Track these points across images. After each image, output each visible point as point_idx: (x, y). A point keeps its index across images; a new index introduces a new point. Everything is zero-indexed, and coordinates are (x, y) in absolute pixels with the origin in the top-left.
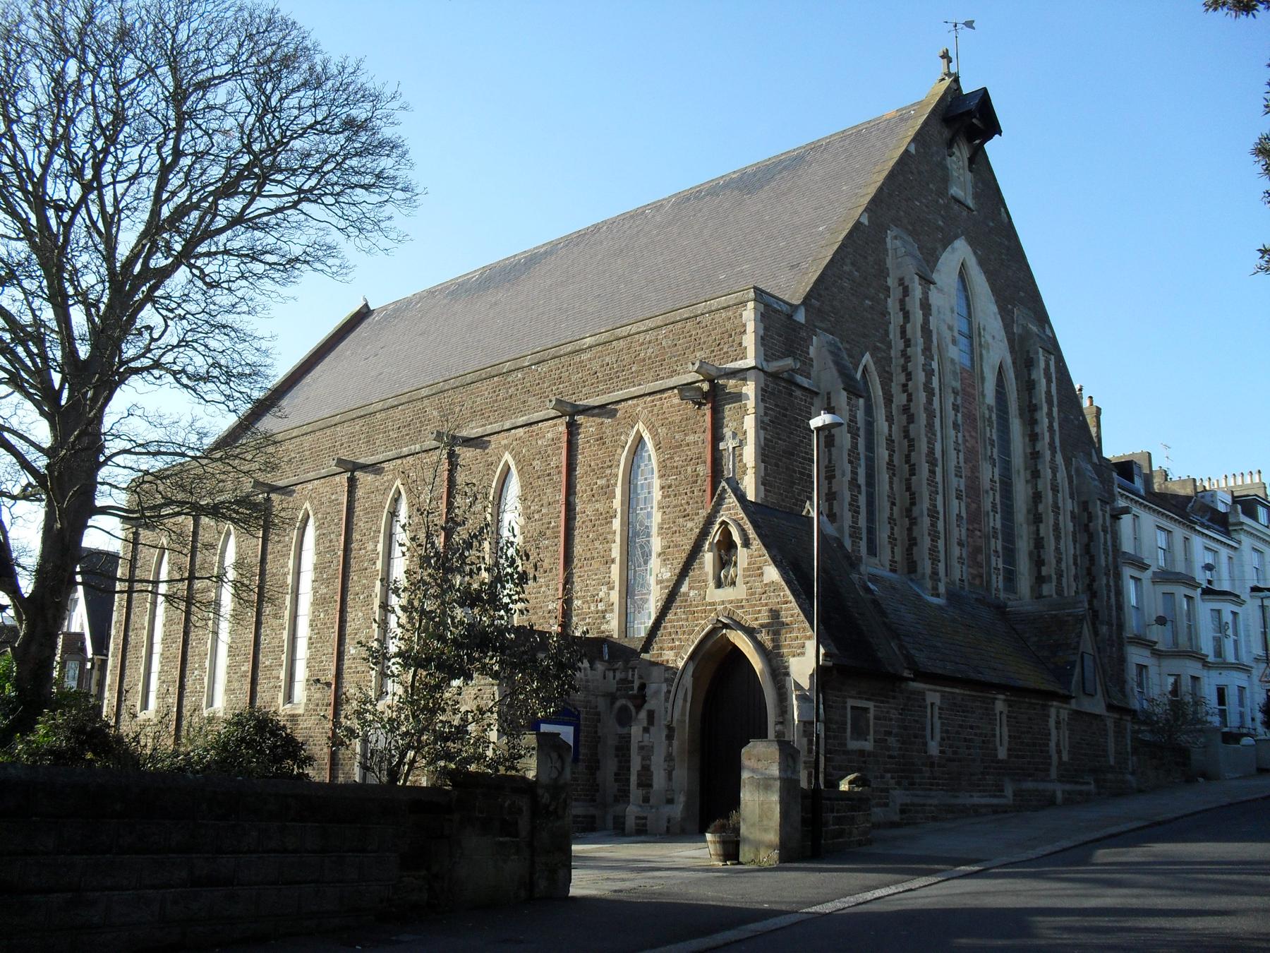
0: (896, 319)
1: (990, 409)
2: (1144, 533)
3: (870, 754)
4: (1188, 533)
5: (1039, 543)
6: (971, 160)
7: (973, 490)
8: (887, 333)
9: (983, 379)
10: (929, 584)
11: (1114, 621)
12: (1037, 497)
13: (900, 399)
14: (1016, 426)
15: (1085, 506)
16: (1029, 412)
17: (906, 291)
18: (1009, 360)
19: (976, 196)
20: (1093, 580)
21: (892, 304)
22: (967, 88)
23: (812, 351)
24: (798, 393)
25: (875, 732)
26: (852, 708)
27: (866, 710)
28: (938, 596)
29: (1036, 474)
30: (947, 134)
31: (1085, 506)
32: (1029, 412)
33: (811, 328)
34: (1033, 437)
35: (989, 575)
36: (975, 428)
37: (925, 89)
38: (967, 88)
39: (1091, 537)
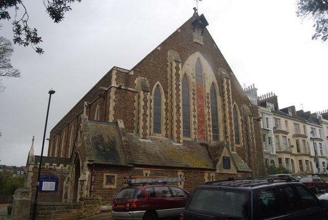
0: (169, 72)
1: (208, 94)
2: (269, 122)
3: (114, 189)
4: (304, 124)
5: (226, 128)
6: (202, 33)
7: (201, 115)
8: (167, 76)
9: (205, 86)
10: (176, 140)
11: (255, 147)
12: (225, 116)
13: (170, 93)
14: (219, 98)
15: (245, 118)
16: (222, 94)
17: (172, 65)
18: (216, 81)
19: (204, 41)
20: (248, 137)
21: (168, 69)
22: (200, 14)
23: (136, 82)
24: (129, 92)
25: (117, 183)
26: (106, 176)
27: (114, 176)
28: (180, 143)
29: (224, 110)
30: (193, 27)
31: (245, 118)
32: (222, 94)
33: (135, 76)
34: (224, 100)
35: (207, 137)
36: (203, 99)
37: (190, 15)
38: (200, 14)
39: (247, 125)
